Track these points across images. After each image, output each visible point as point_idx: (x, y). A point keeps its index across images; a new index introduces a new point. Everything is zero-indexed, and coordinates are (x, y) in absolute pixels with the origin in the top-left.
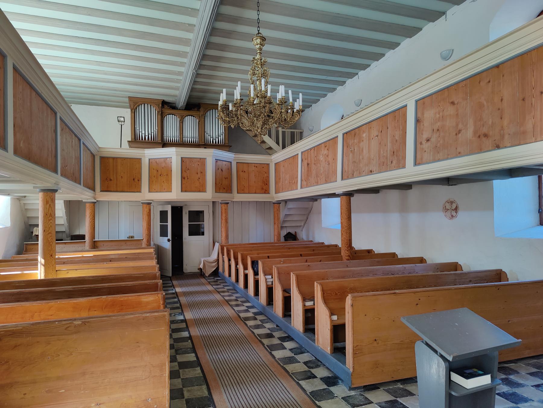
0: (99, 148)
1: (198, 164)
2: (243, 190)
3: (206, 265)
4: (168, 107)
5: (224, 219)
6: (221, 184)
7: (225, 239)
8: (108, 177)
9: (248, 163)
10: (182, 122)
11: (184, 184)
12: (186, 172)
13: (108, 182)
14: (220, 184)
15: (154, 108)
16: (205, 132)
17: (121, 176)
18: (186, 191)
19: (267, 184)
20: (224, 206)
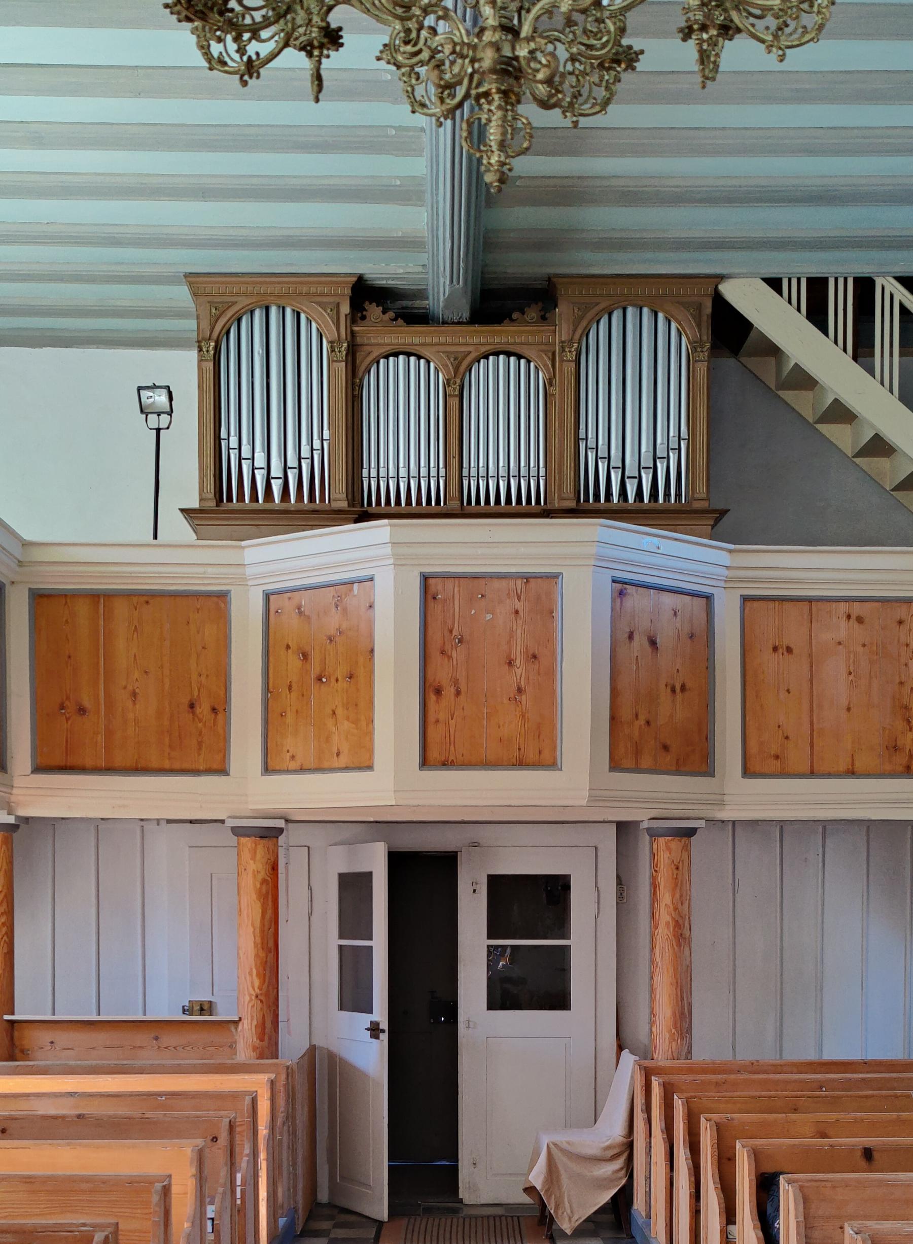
0: (26, 544)
1: (517, 612)
3: (562, 1171)
4: (384, 313)
5: (667, 924)
6: (648, 723)
7: (672, 1035)
8: (68, 698)
9: (810, 600)
11: (437, 721)
12: (450, 657)
13: (67, 719)
14: (642, 721)
15: (314, 325)
16: (577, 440)
17: (130, 688)
18: (446, 764)
20: (669, 849)
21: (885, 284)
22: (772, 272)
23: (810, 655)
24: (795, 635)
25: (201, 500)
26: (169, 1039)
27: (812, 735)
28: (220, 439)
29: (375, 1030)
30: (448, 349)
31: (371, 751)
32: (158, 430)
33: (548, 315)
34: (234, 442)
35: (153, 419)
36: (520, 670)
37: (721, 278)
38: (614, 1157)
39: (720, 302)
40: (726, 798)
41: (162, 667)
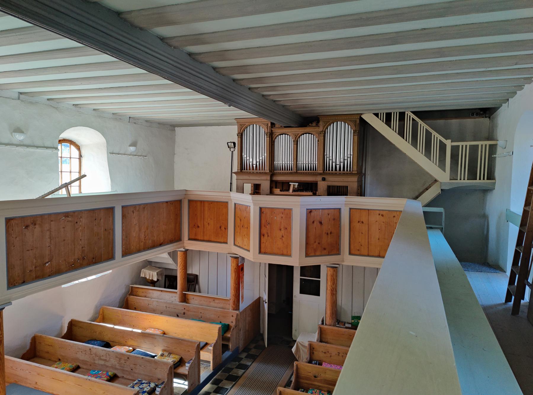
1: (282, 217)
2: (359, 250)
6: (319, 243)
9: (368, 210)
10: (296, 143)
11: (263, 242)
12: (266, 227)
14: (317, 243)
17: (208, 222)
18: (265, 253)
20: (330, 271)
21: (408, 113)
22: (376, 112)
23: (368, 224)
24: (364, 219)
27: (368, 245)
28: (242, 155)
33: (318, 124)
34: (245, 156)
36: (283, 231)
37: (362, 114)
39: (362, 120)
40: (344, 260)
41: (214, 218)
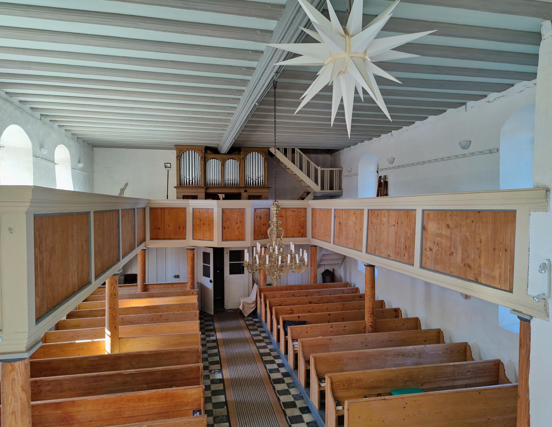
6: (260, 231)
9: (286, 208)
10: (223, 165)
12: (227, 222)
14: (259, 231)
16: (245, 174)
17: (168, 224)
18: (226, 240)
19: (304, 228)
25: (177, 185)
26: (174, 286)
29: (211, 281)
30: (221, 158)
31: (213, 238)
32: (168, 170)
34: (183, 174)
35: (167, 169)
36: (239, 224)
38: (254, 303)
